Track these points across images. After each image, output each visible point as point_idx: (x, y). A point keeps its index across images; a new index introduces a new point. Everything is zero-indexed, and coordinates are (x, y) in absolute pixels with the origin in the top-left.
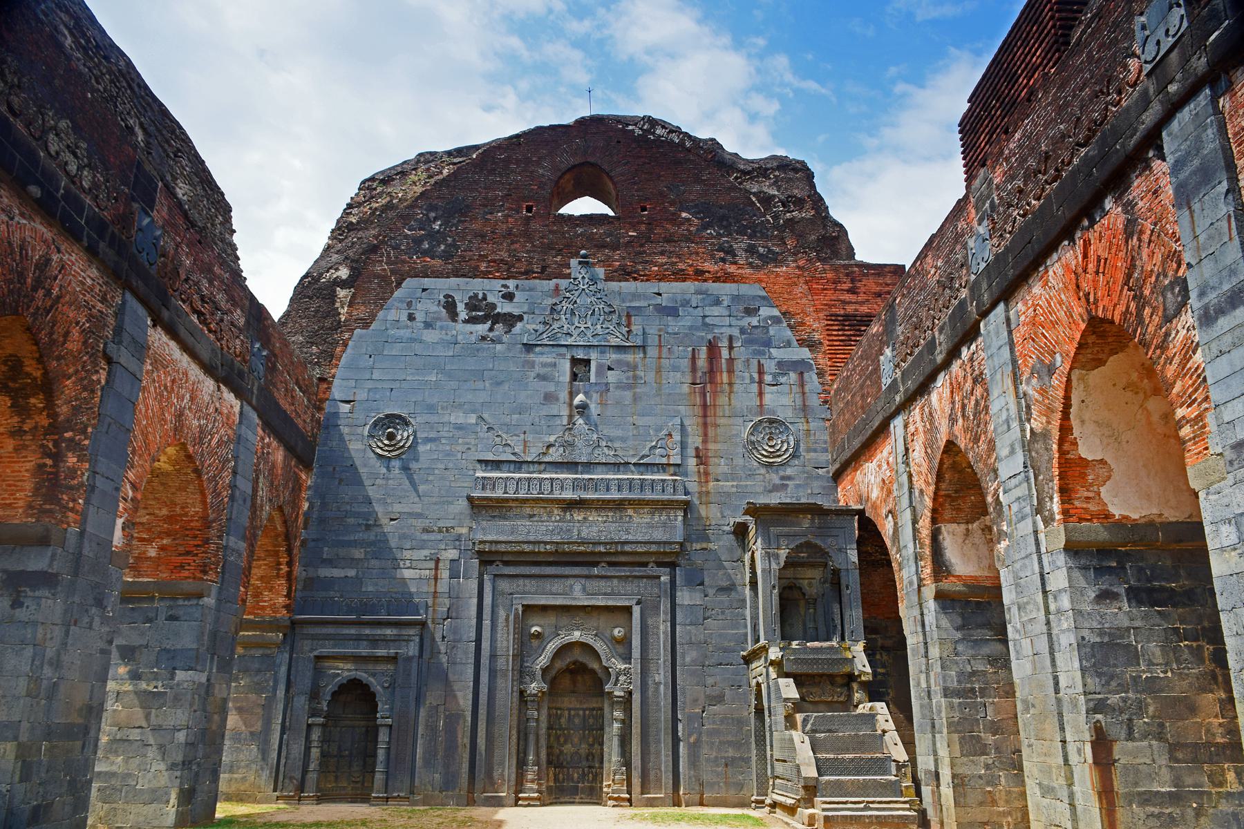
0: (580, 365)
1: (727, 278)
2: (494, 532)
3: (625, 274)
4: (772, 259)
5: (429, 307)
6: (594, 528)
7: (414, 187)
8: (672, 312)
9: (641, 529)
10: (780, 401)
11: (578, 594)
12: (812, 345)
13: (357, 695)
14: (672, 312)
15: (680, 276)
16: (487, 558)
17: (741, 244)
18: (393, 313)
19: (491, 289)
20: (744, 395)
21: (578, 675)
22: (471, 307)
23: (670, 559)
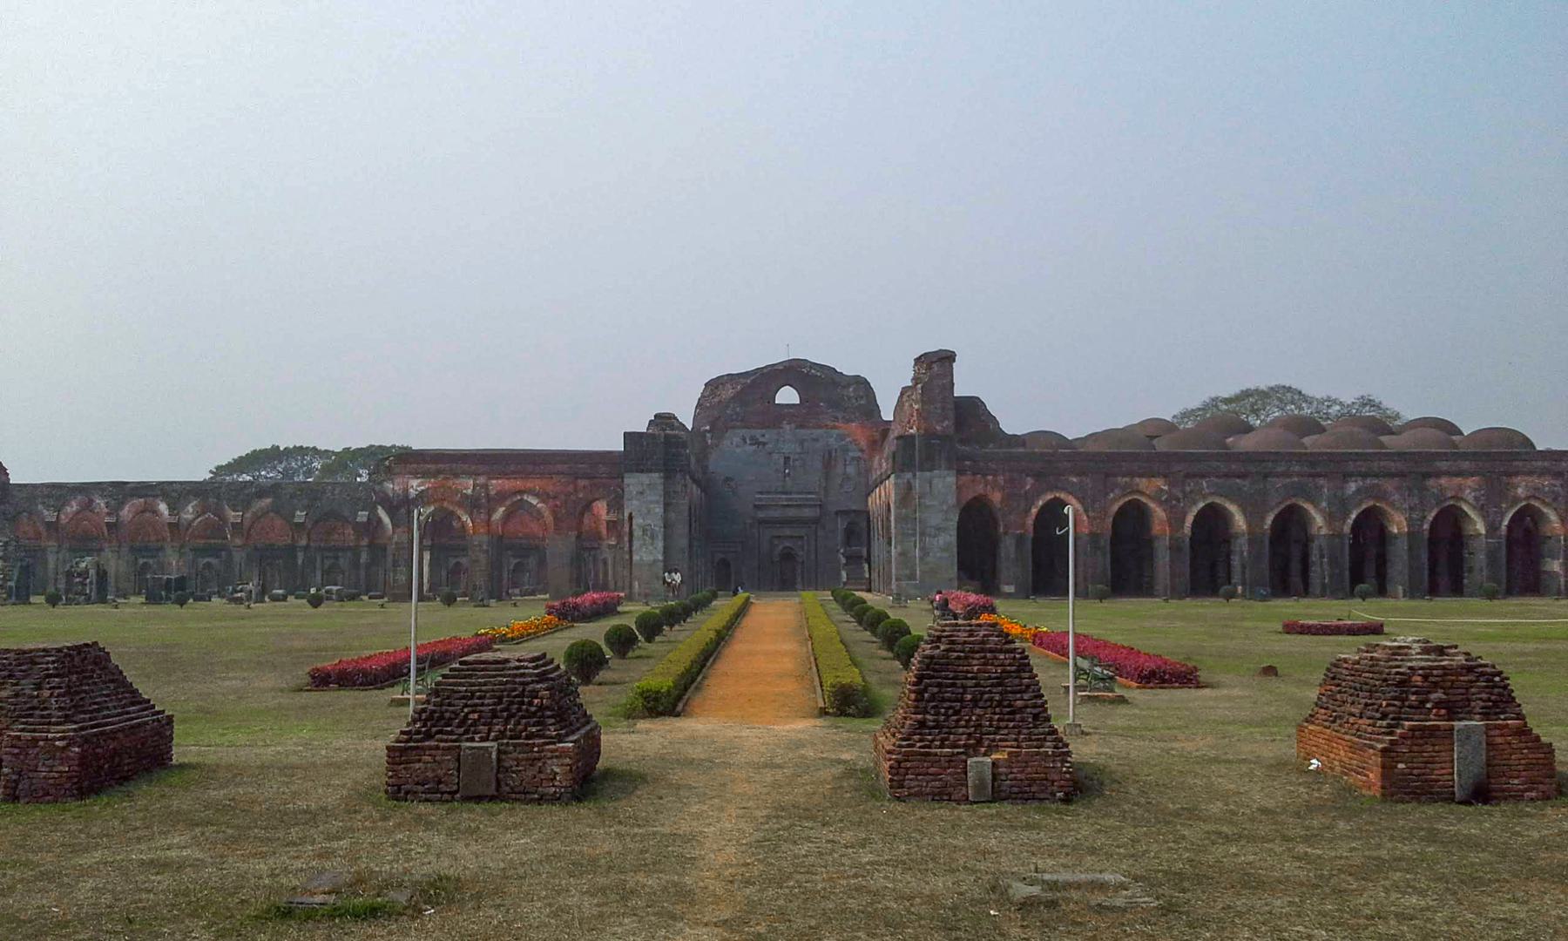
0: (787, 459)
1: (834, 427)
2: (761, 515)
3: (801, 426)
4: (849, 421)
5: (736, 440)
6: (792, 513)
7: (728, 392)
8: (816, 440)
9: (807, 513)
10: (851, 470)
11: (788, 532)
12: (862, 451)
13: (725, 564)
14: (816, 440)
15: (820, 427)
16: (762, 522)
17: (840, 415)
18: (726, 442)
19: (757, 433)
20: (839, 469)
21: (788, 556)
22: (752, 438)
23: (816, 521)
